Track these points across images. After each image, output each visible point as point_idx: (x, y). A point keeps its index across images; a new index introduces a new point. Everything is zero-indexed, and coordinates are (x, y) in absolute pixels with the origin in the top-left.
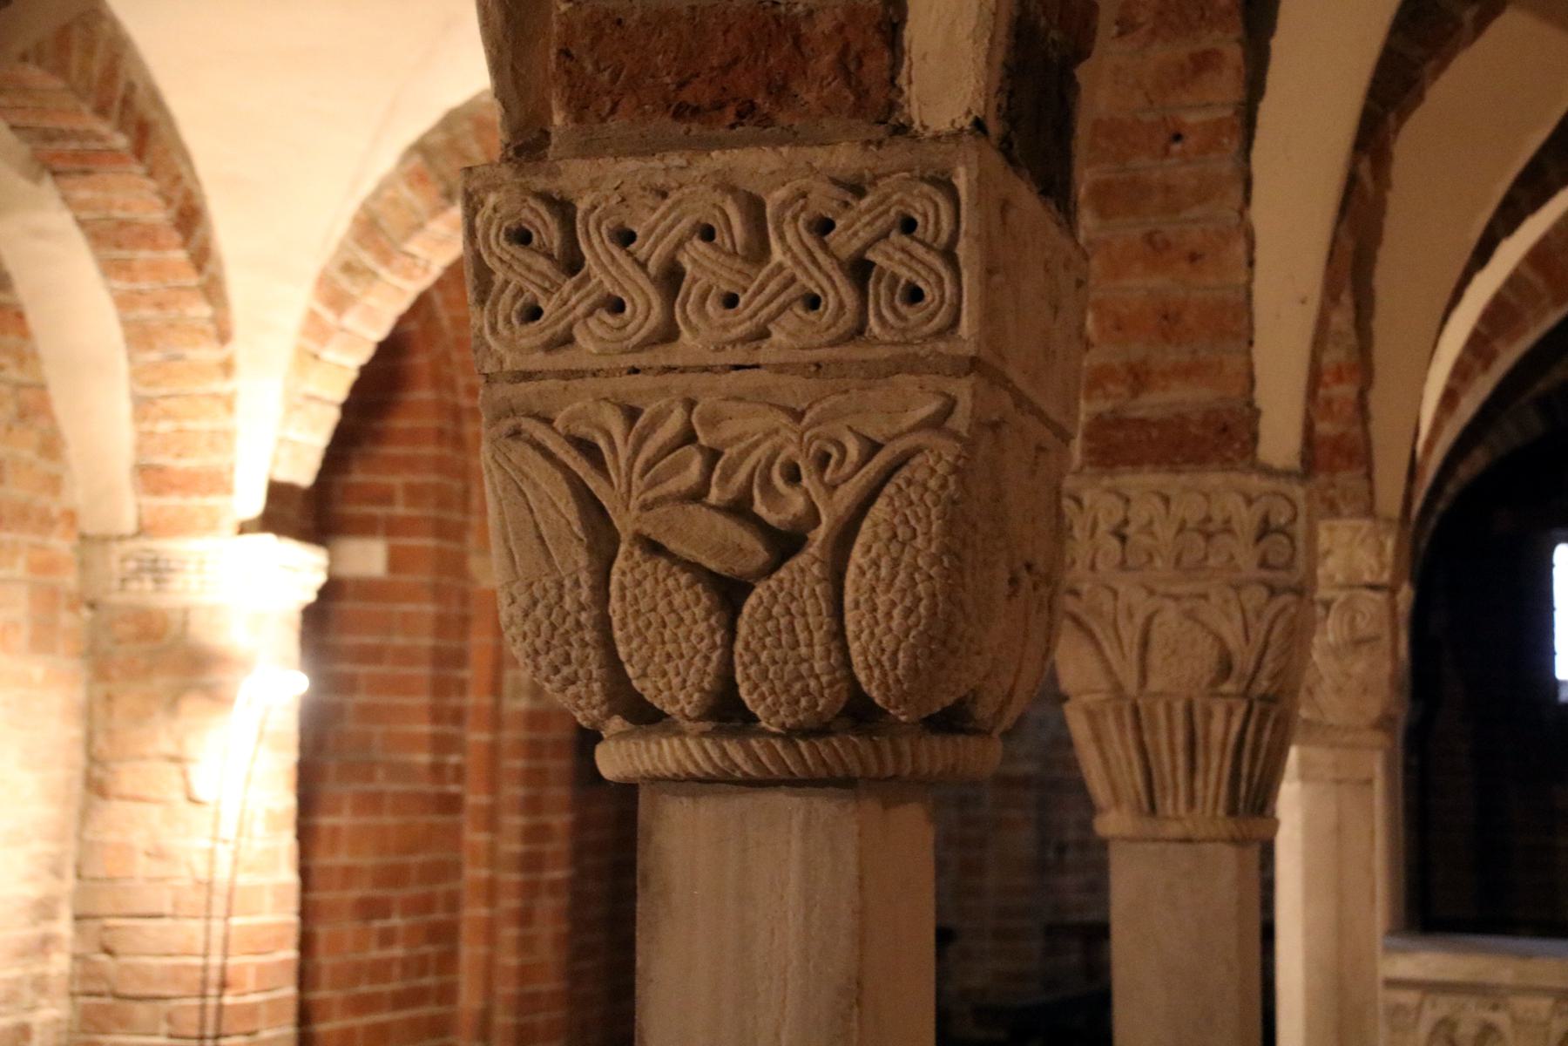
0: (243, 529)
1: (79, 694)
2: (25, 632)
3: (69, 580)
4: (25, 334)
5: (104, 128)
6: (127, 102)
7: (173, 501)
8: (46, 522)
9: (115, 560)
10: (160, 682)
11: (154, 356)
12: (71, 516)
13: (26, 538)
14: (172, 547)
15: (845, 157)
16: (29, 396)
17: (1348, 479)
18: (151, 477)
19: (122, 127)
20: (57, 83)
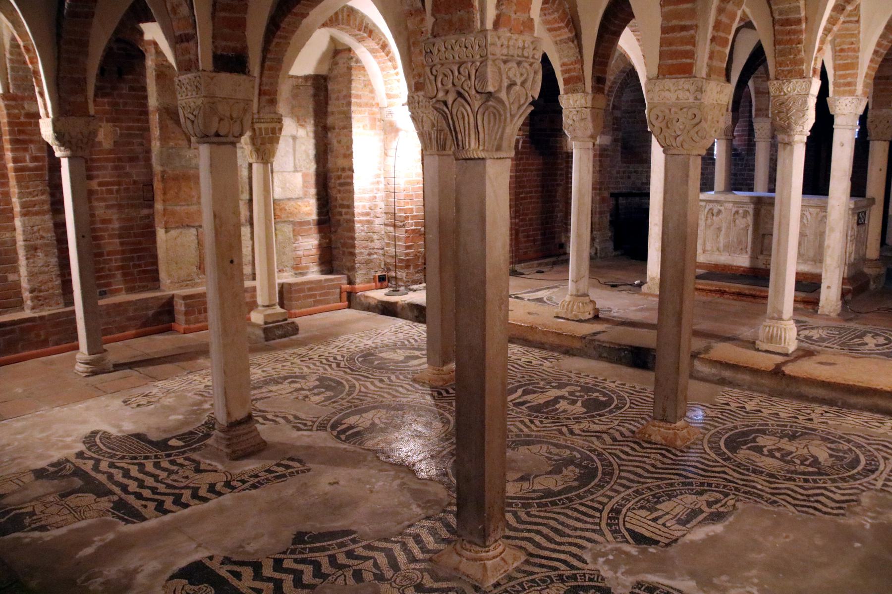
0: (403, 105)
1: (382, 137)
2: (369, 125)
3: (378, 116)
4: (365, 71)
5: (361, 33)
6: (366, 27)
7: (392, 100)
8: (372, 105)
9: (385, 112)
10: (393, 134)
11: (385, 73)
12: (378, 104)
13: (367, 109)
14: (392, 109)
15: (194, 74)
16: (367, 82)
17: (580, 85)
18: (389, 96)
19: (365, 32)
20: (348, 27)
